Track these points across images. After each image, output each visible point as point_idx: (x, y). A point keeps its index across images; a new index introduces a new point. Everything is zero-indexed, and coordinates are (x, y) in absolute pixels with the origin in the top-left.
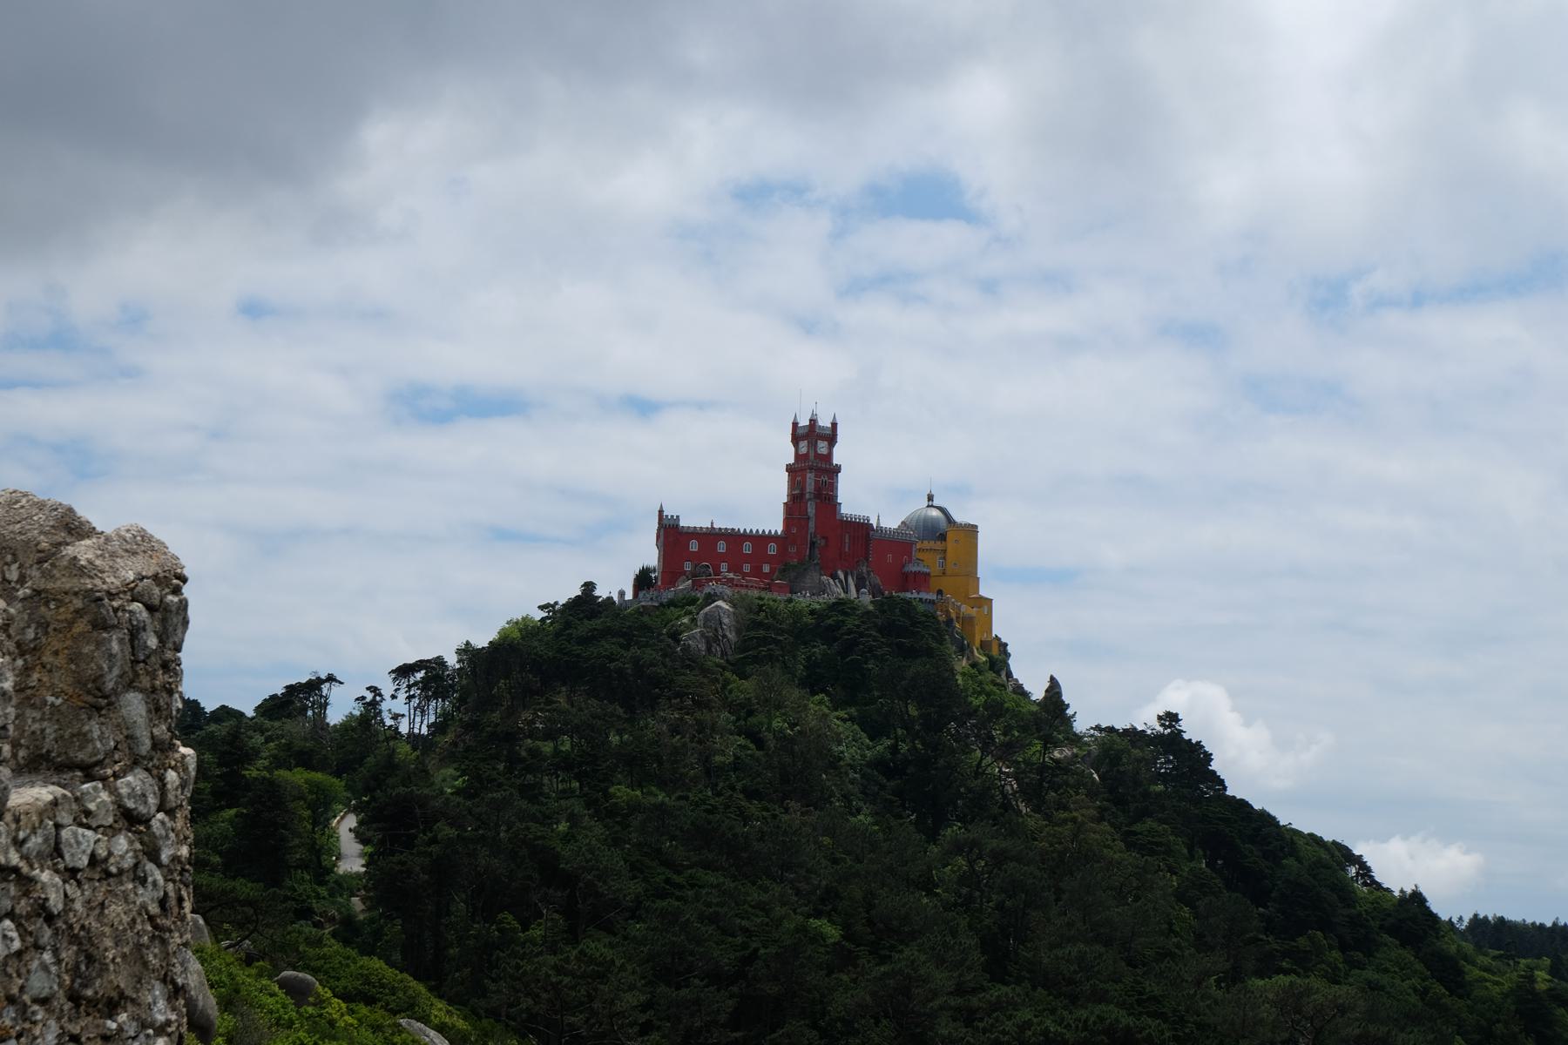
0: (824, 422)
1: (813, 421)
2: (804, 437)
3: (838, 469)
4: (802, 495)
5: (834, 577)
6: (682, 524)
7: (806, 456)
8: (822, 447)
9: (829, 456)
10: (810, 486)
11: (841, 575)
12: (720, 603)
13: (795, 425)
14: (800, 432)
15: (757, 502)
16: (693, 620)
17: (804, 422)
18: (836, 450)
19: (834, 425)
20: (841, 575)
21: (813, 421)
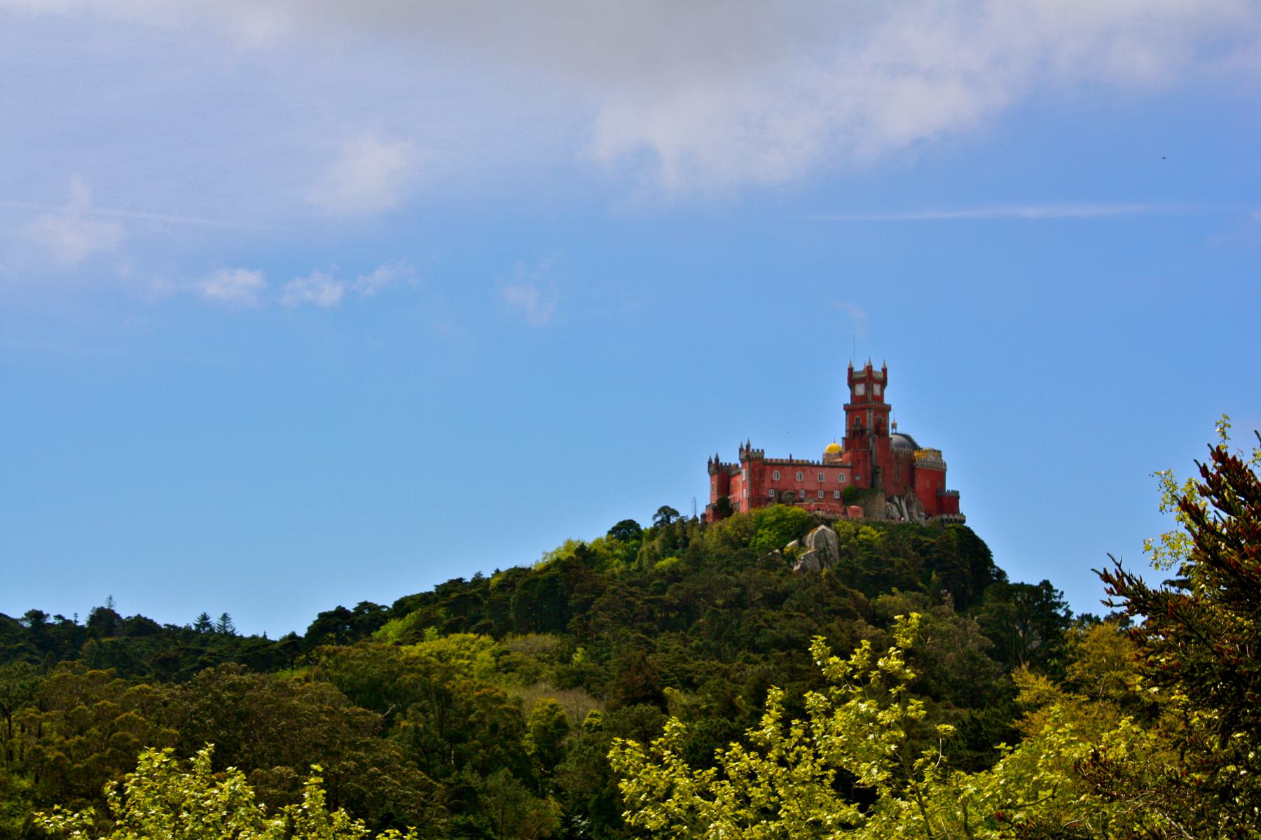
0: (877, 368)
1: (869, 369)
2: (861, 381)
3: (888, 408)
4: (863, 431)
5: (890, 500)
6: (767, 456)
7: (864, 398)
8: (877, 389)
9: (881, 398)
10: (870, 425)
11: (897, 500)
12: (823, 527)
13: (850, 370)
14: (856, 376)
15: (817, 436)
16: (802, 544)
17: (859, 367)
18: (886, 391)
19: (885, 370)
20: (897, 500)
21: (869, 369)
